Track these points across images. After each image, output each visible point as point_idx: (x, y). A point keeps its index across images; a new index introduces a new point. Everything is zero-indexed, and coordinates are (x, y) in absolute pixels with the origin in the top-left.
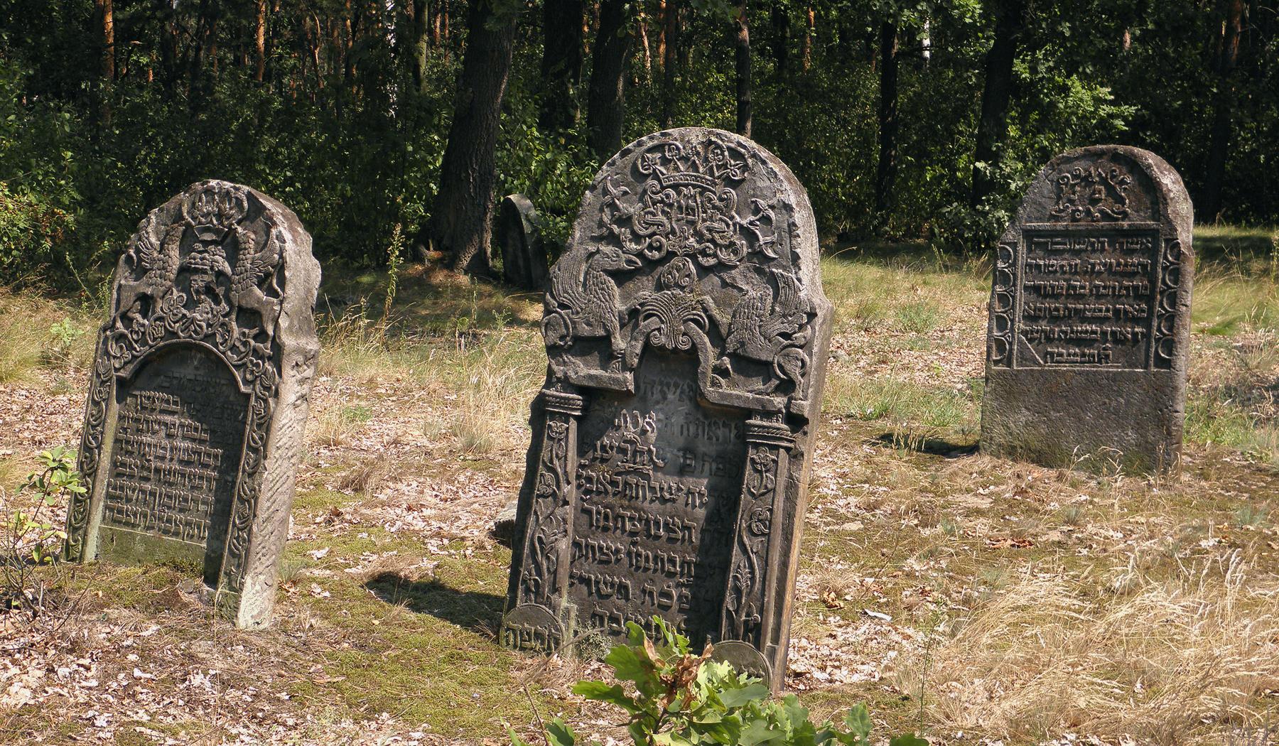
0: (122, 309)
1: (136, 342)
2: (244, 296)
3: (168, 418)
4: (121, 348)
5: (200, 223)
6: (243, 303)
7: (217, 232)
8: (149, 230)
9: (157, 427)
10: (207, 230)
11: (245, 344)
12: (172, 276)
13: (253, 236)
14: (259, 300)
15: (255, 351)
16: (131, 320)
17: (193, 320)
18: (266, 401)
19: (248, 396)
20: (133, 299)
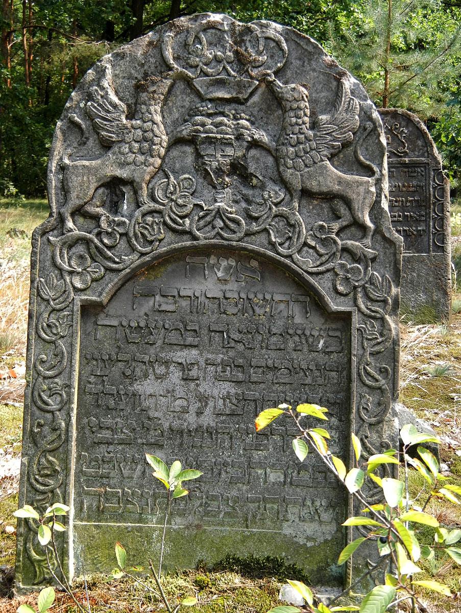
0: (74, 202)
1: (110, 248)
2: (310, 176)
3: (181, 356)
4: (81, 257)
5: (206, 75)
6: (313, 185)
7: (240, 86)
8: (105, 84)
9: (161, 370)
10: (221, 83)
11: (325, 242)
12: (163, 151)
13: (306, 92)
14: (340, 181)
15: (345, 250)
16: (96, 218)
17: (219, 213)
18: (382, 319)
19: (345, 318)
20: (93, 186)
